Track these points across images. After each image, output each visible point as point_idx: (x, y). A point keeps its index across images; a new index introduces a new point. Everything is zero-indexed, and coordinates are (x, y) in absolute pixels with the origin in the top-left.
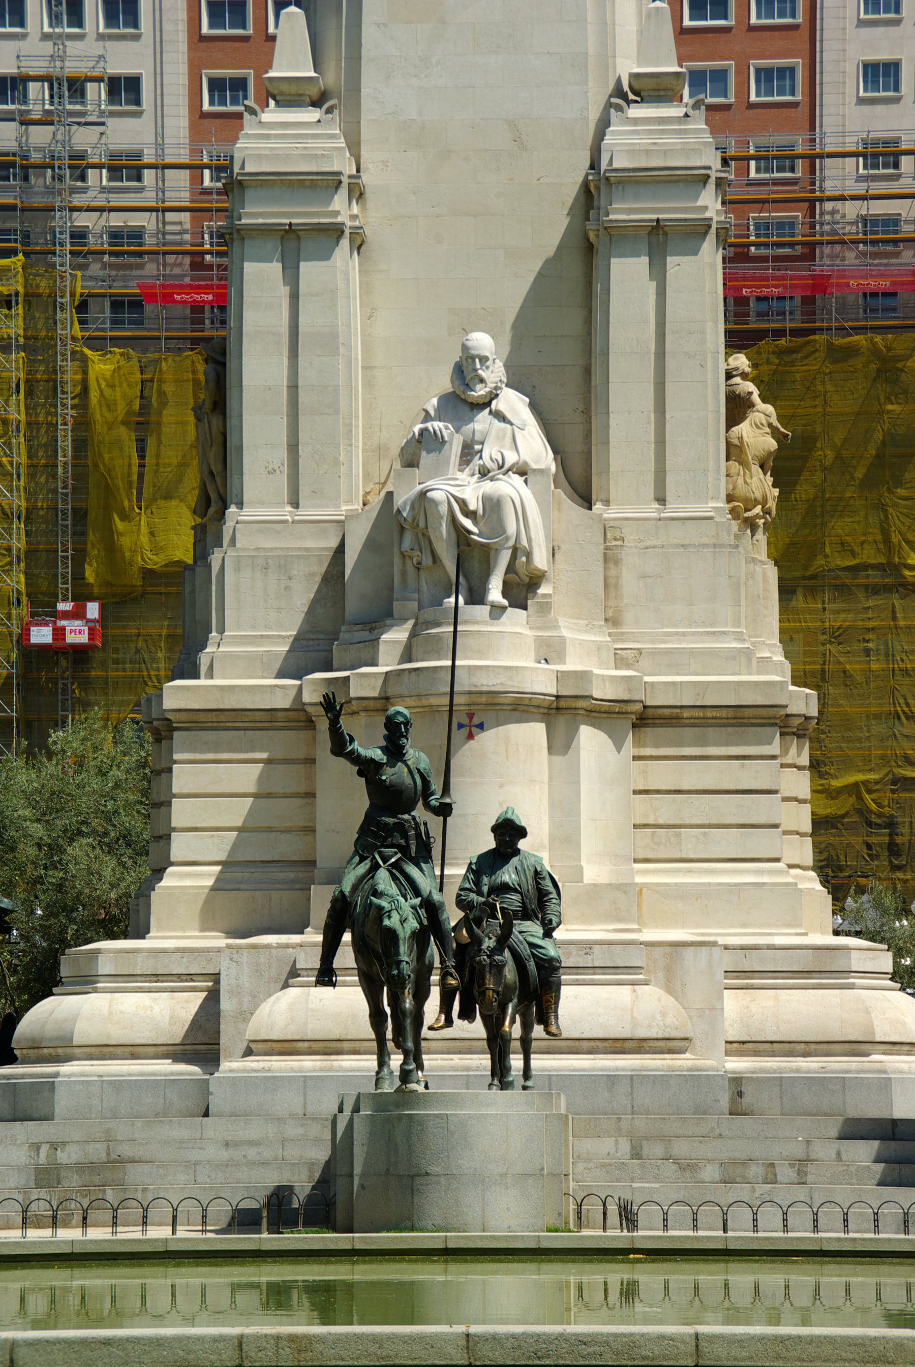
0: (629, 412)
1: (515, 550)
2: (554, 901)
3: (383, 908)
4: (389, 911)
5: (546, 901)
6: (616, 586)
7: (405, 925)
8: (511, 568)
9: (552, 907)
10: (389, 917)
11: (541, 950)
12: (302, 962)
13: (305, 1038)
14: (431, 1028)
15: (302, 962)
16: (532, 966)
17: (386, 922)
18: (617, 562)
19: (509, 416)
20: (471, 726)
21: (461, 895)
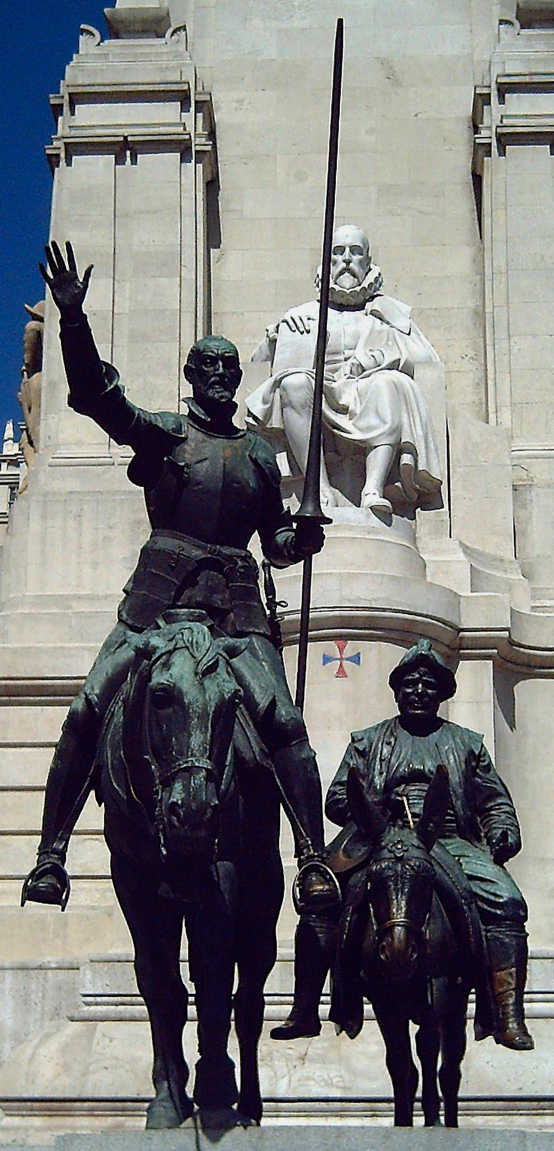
0: (534, 335)
1: (399, 449)
2: (507, 809)
3: (155, 648)
4: (170, 653)
5: (491, 809)
6: (524, 534)
7: (207, 683)
8: (393, 473)
9: (499, 819)
10: (167, 666)
11: (488, 887)
12: (88, 986)
13: (84, 1095)
14: (277, 1034)
15: (88, 986)
16: (471, 914)
17: (159, 678)
18: (524, 506)
19: (387, 318)
20: (341, 659)
21: (335, 793)
